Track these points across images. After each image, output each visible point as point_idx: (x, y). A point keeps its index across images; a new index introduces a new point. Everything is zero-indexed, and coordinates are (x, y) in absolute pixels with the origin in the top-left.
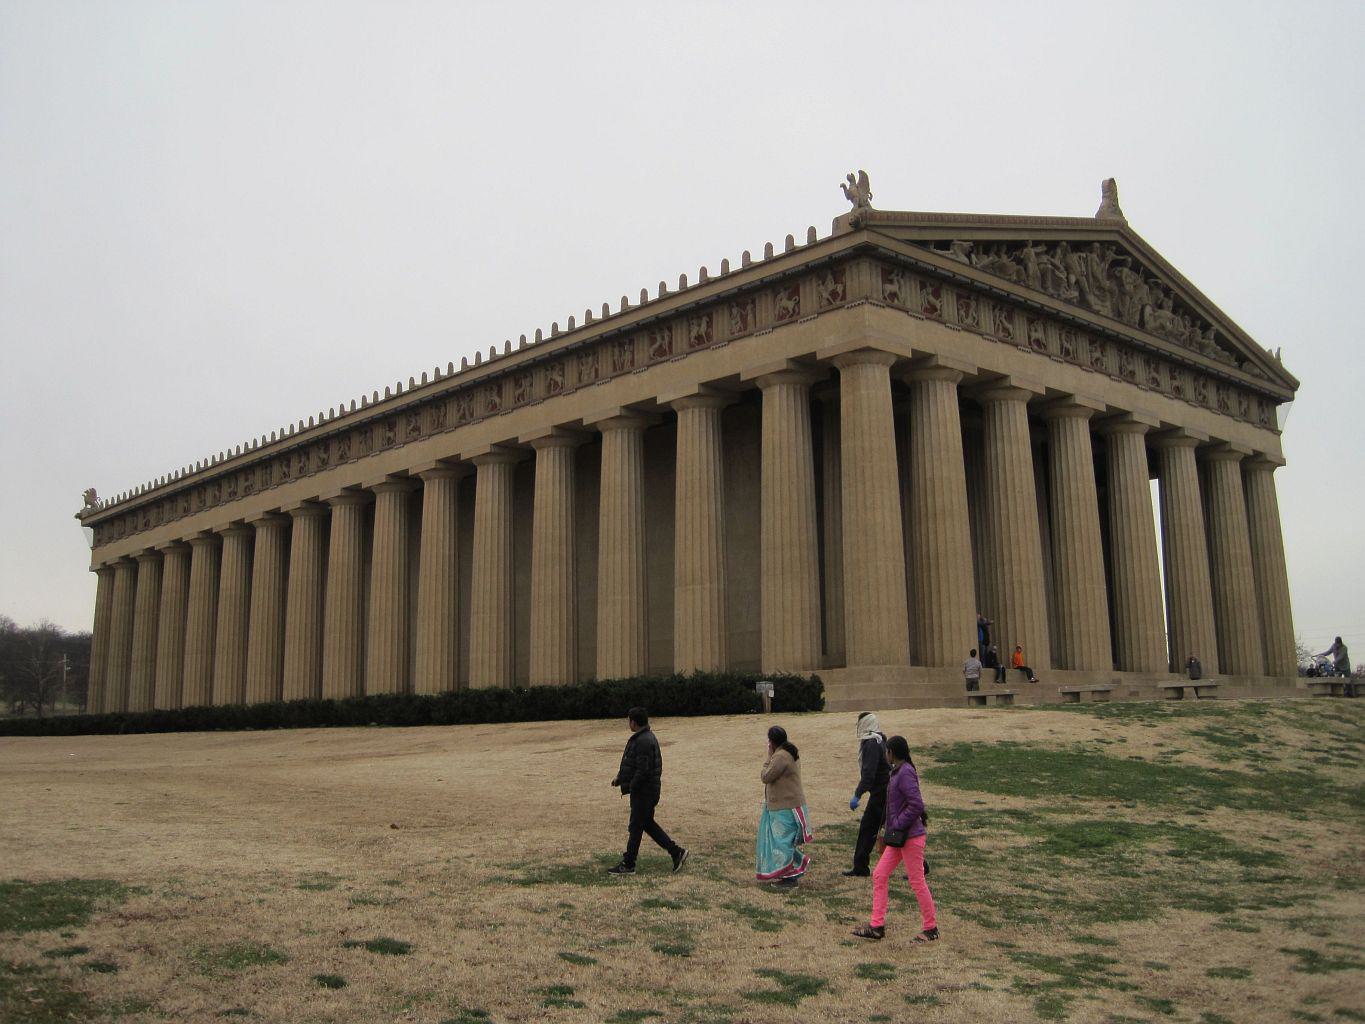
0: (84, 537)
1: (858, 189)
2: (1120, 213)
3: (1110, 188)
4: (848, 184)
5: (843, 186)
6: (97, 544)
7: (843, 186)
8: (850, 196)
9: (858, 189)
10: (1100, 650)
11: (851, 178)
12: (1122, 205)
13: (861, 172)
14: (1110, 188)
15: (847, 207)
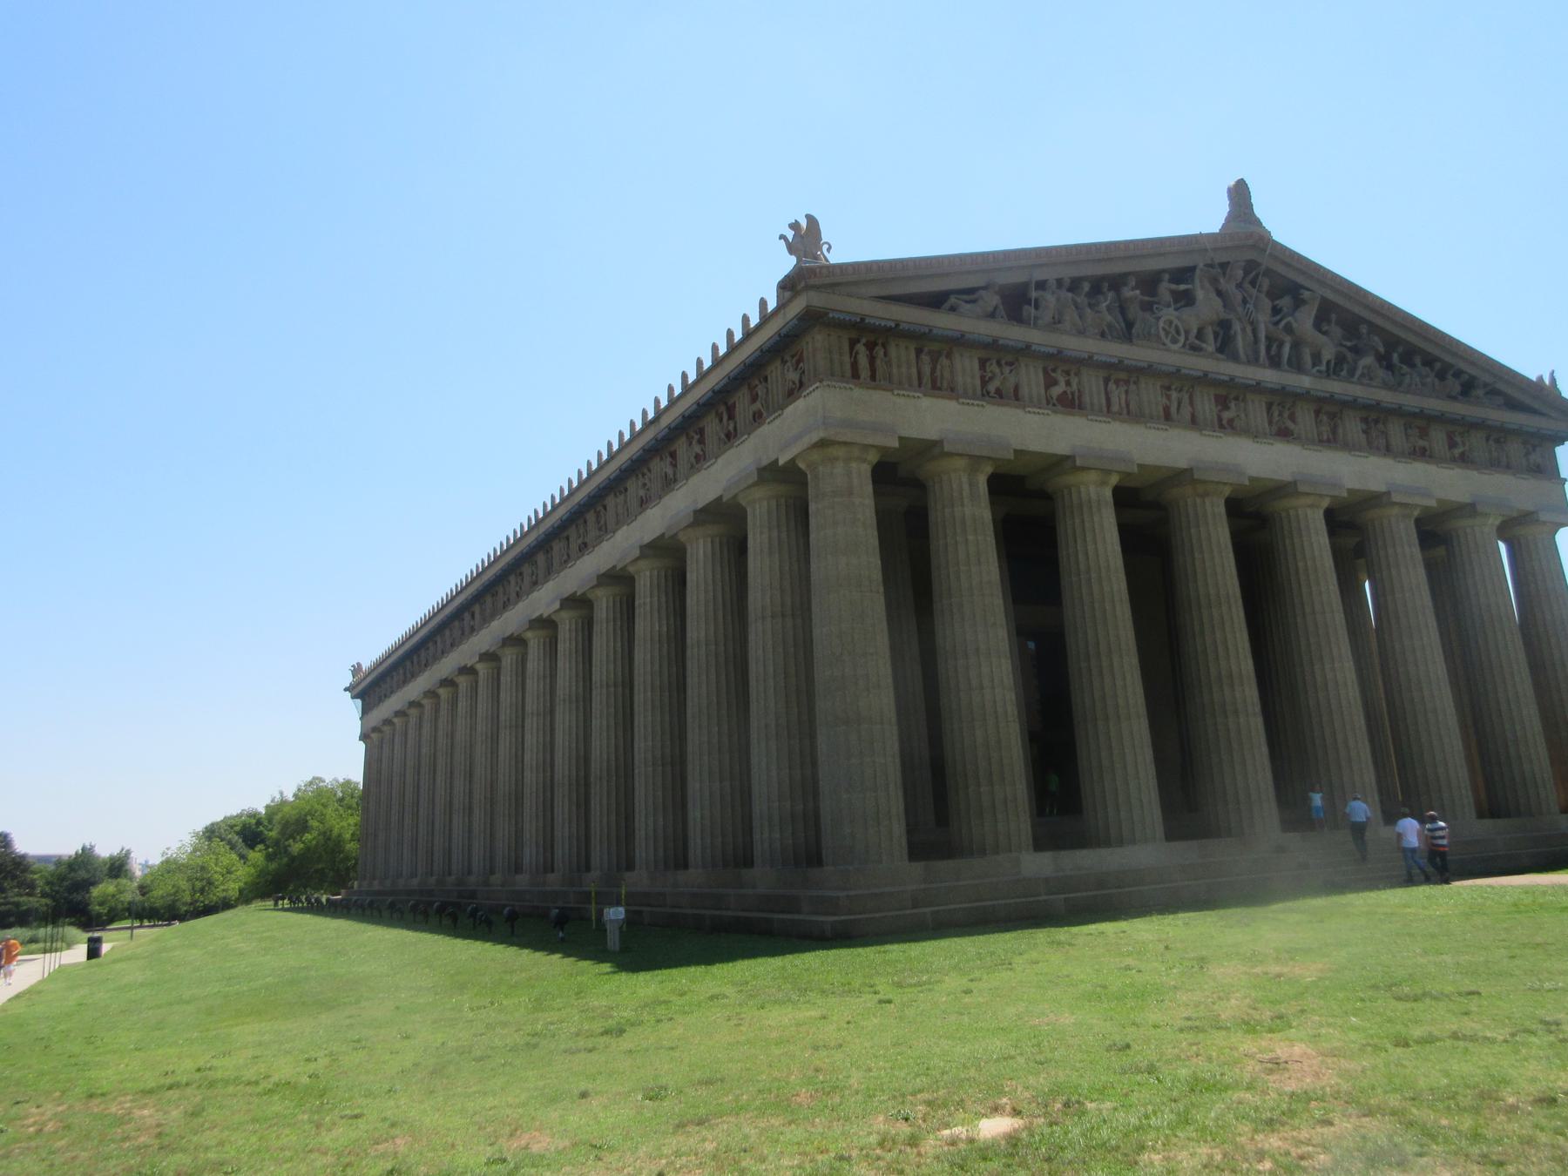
0: (353, 708)
1: (805, 238)
2: (1258, 222)
3: (1240, 194)
4: (790, 234)
5: (782, 237)
6: (365, 711)
7: (782, 237)
8: (791, 249)
9: (805, 238)
10: (581, 1043)
11: (795, 226)
12: (1259, 211)
13: (811, 220)
14: (1240, 194)
15: (788, 263)
